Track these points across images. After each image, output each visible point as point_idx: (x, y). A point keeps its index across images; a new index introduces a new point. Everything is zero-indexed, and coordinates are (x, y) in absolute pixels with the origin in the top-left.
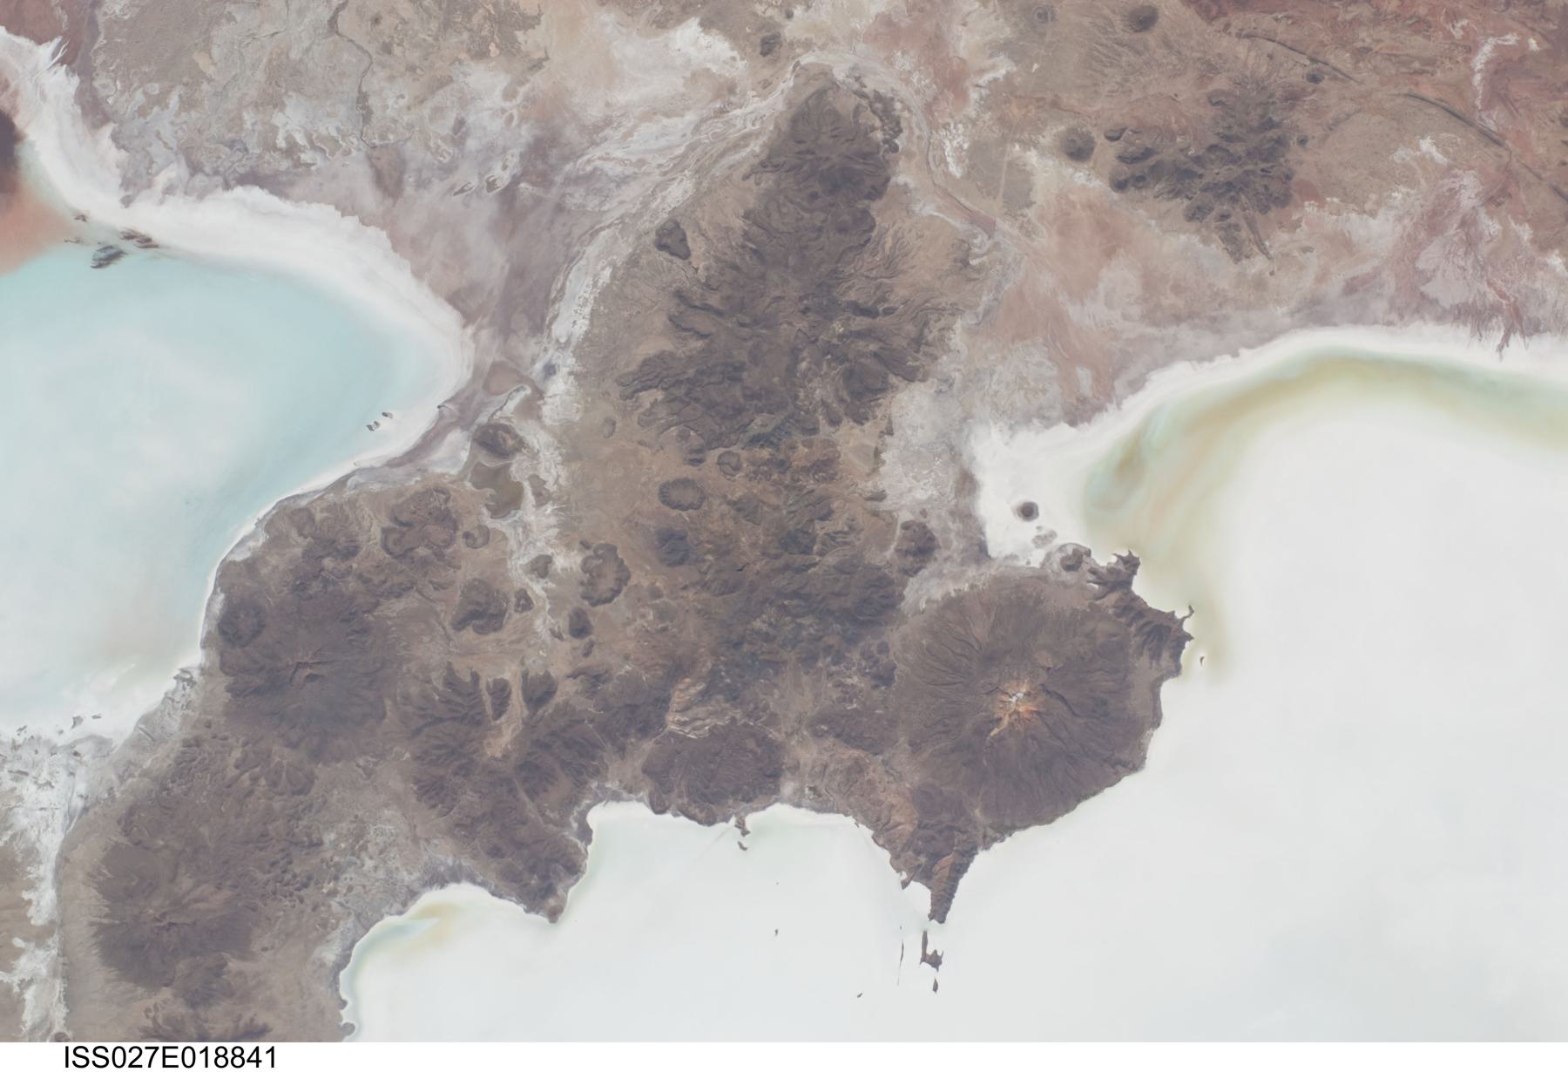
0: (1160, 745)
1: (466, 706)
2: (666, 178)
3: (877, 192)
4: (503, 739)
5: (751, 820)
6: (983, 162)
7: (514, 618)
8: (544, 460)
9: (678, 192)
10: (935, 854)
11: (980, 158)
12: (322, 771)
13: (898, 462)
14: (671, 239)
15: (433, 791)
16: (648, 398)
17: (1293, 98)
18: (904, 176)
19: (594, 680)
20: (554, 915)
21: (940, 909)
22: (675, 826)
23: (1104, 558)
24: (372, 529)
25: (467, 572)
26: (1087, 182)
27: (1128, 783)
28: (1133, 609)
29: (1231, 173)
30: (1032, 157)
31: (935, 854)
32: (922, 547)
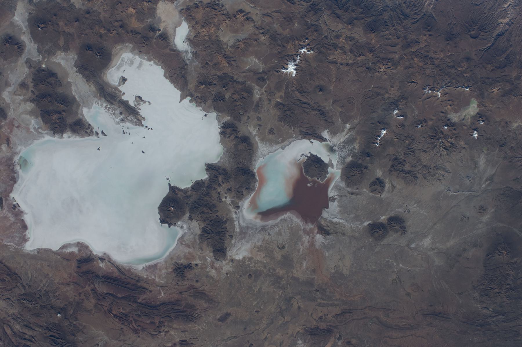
0: (157, 211)
1: (227, 180)
2: (235, 243)
3: (214, 251)
4: (220, 179)
5: (192, 184)
6: (204, 259)
7: (226, 191)
8: (231, 208)
9: (233, 242)
10: (173, 189)
11: (206, 260)
12: (236, 166)
14: (231, 236)
15: (224, 170)
16: (225, 219)
17: (178, 280)
18: (211, 254)
19: (215, 189)
20: (206, 164)
21: (169, 184)
22: (199, 179)
23: (172, 226)
24: (245, 192)
25: (233, 193)
26: (194, 262)
27: (158, 206)
28: (167, 223)
29: (181, 269)
30: (200, 262)
31: (173, 189)
32: (190, 218)
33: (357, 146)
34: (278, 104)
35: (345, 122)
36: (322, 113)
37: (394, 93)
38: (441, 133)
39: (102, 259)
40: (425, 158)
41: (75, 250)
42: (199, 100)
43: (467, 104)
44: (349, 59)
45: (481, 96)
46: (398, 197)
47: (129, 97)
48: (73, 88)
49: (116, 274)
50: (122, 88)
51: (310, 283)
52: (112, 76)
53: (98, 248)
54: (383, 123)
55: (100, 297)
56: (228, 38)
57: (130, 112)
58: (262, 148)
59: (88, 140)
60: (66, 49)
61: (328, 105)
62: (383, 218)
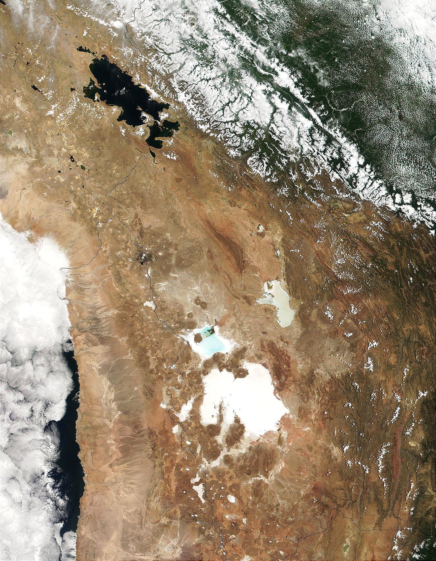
10: (236, 377)
13: (241, 362)
33: (183, 330)
34: (187, 363)
35: (177, 339)
36: (180, 348)
37: (159, 331)
38: (161, 307)
39: (274, 384)
40: (172, 307)
41: (277, 394)
42: (202, 388)
43: (147, 306)
44: (158, 351)
45: (142, 304)
46: (189, 307)
47: (217, 411)
48: (226, 431)
49: (275, 377)
50: (215, 415)
51: (235, 315)
52: (214, 421)
53: (272, 388)
54: (170, 327)
55: (287, 377)
56: (178, 392)
57: (221, 407)
58: (203, 360)
59: (239, 416)
60: (216, 441)
61: (177, 348)
62: (199, 306)
